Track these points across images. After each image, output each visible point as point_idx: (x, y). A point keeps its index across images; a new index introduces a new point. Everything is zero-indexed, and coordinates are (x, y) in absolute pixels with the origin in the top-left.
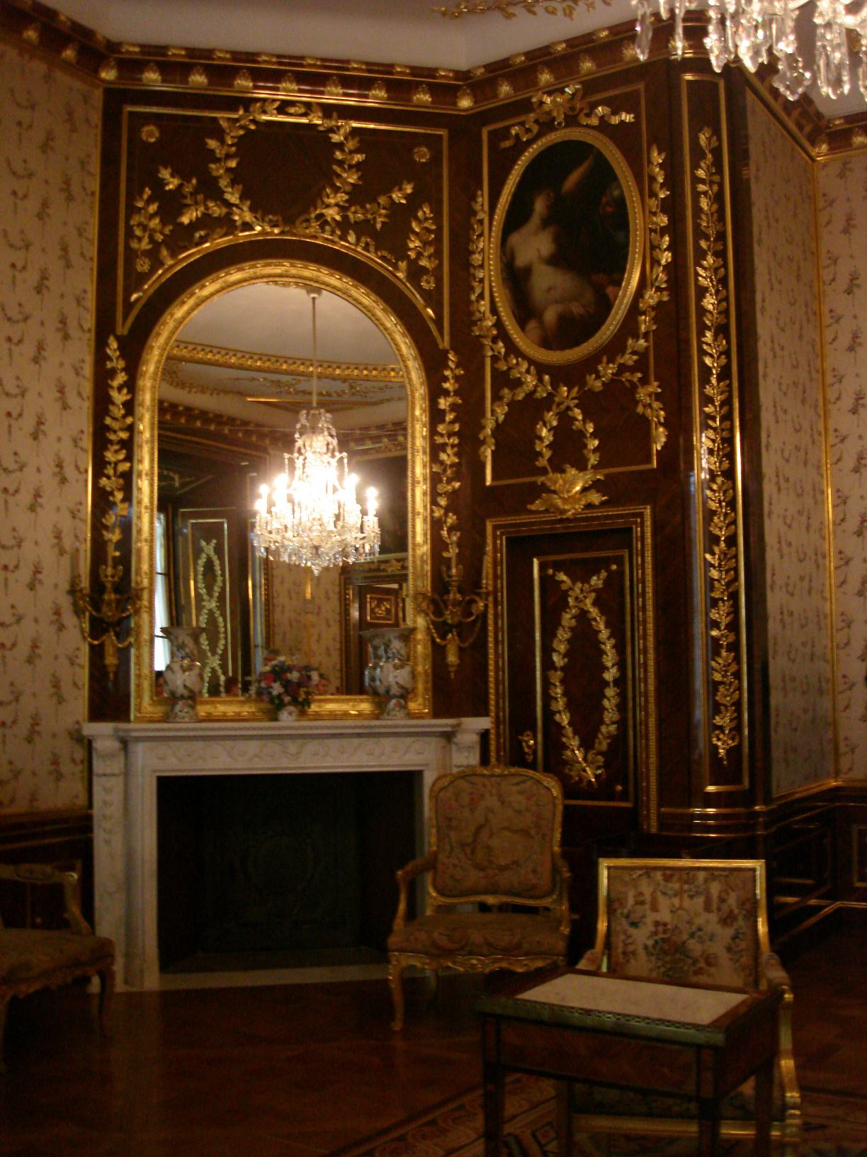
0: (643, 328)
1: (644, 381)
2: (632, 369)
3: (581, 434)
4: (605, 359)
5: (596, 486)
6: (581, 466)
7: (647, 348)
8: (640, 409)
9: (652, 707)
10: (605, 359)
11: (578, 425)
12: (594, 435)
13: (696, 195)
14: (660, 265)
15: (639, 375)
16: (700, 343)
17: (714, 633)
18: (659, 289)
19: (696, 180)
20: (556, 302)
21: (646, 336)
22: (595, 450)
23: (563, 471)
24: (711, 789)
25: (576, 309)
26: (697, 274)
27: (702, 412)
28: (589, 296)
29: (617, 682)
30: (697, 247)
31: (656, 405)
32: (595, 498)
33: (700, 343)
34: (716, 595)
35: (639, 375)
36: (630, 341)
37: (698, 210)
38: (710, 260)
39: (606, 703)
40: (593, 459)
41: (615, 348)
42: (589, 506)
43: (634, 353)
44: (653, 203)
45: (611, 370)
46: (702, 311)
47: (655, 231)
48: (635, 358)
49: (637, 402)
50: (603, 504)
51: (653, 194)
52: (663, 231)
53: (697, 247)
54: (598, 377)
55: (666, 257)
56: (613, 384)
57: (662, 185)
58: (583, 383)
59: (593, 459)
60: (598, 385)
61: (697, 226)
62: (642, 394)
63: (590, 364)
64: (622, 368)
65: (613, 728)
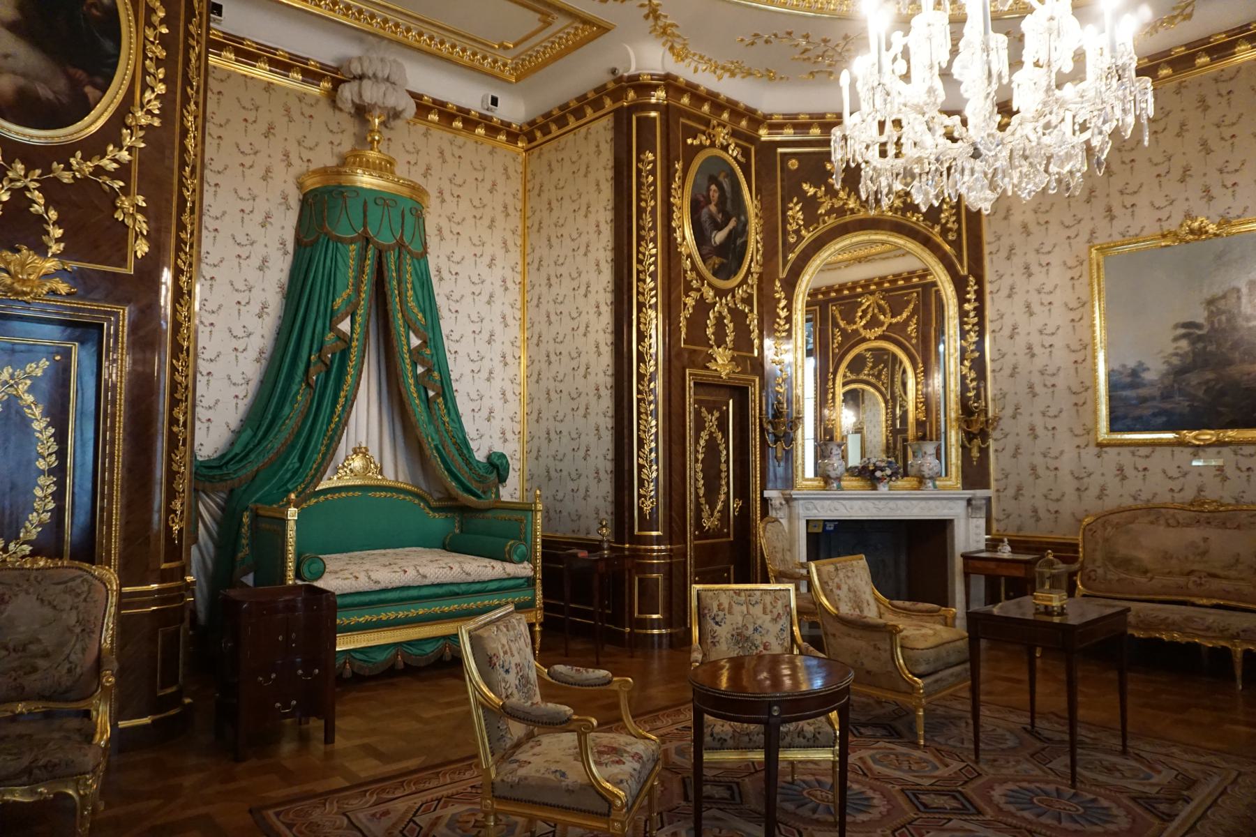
0: (128, 142)
1: (126, 191)
2: (114, 175)
3: (40, 219)
4: (79, 154)
5: (60, 274)
6: (42, 250)
7: (130, 161)
8: (119, 216)
9: (117, 494)
10: (79, 154)
11: (36, 208)
12: (57, 223)
13: (188, 47)
14: (153, 91)
15: (122, 184)
16: (181, 176)
17: (175, 429)
18: (149, 112)
19: (188, 34)
20: (14, 73)
21: (130, 149)
22: (58, 241)
23: (18, 251)
24: (164, 566)
25: (43, 91)
26: (183, 116)
27: (178, 236)
28: (62, 84)
29: (51, 472)
30: (184, 91)
31: (139, 217)
32: (63, 288)
33: (181, 176)
34: (178, 396)
35: (122, 184)
36: (111, 148)
37: (187, 61)
38: (193, 107)
39: (38, 492)
40: (55, 248)
41: (93, 146)
42: (53, 292)
43: (114, 160)
44: (150, 33)
45: (88, 167)
46: (184, 149)
47: (151, 59)
48: (115, 165)
49: (116, 208)
50: (68, 294)
51: (149, 24)
52: (159, 63)
53: (184, 91)
54: (68, 167)
55: (161, 88)
56: (82, 184)
57: (162, 21)
58: (48, 169)
59: (55, 248)
60: (67, 178)
61: (185, 74)
62: (125, 202)
63: (63, 153)
64: (99, 171)
65: (46, 517)
